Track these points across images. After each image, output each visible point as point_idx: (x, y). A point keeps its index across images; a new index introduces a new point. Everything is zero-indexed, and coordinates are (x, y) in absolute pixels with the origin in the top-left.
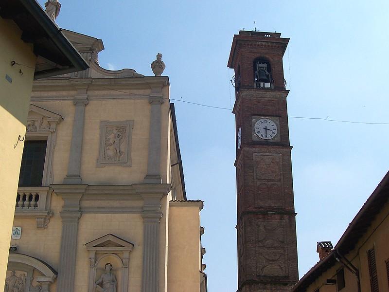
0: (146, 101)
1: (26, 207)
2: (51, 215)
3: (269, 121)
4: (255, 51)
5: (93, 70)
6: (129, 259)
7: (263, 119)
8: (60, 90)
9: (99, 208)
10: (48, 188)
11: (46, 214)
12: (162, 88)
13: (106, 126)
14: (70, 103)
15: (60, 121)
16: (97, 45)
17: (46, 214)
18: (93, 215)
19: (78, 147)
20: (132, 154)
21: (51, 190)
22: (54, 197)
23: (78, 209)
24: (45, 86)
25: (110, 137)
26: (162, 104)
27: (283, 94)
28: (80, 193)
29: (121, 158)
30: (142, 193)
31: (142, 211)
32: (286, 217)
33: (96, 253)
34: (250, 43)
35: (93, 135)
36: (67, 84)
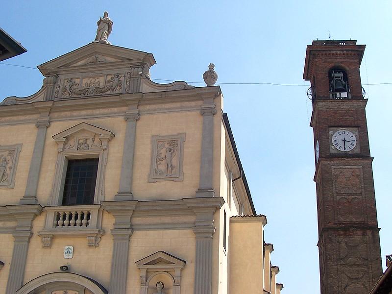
0: (199, 112)
1: (78, 226)
2: (102, 233)
3: (347, 132)
4: (330, 60)
5: (144, 84)
6: (181, 277)
7: (341, 131)
8: (112, 107)
9: (150, 225)
10: (99, 206)
11: (97, 232)
12: (214, 98)
13: (157, 140)
14: (121, 119)
15: (112, 138)
16: (147, 60)
17: (97, 232)
18: (144, 232)
19: (129, 163)
20: (184, 167)
21: (103, 208)
22: (106, 215)
23: (129, 226)
24: (96, 104)
25: (161, 151)
26: (214, 114)
27: (361, 103)
28: (129, 210)
29: (173, 173)
30: (193, 207)
31: (195, 227)
32: (369, 233)
33: (147, 272)
34: (324, 53)
35: (144, 151)
36: (118, 100)
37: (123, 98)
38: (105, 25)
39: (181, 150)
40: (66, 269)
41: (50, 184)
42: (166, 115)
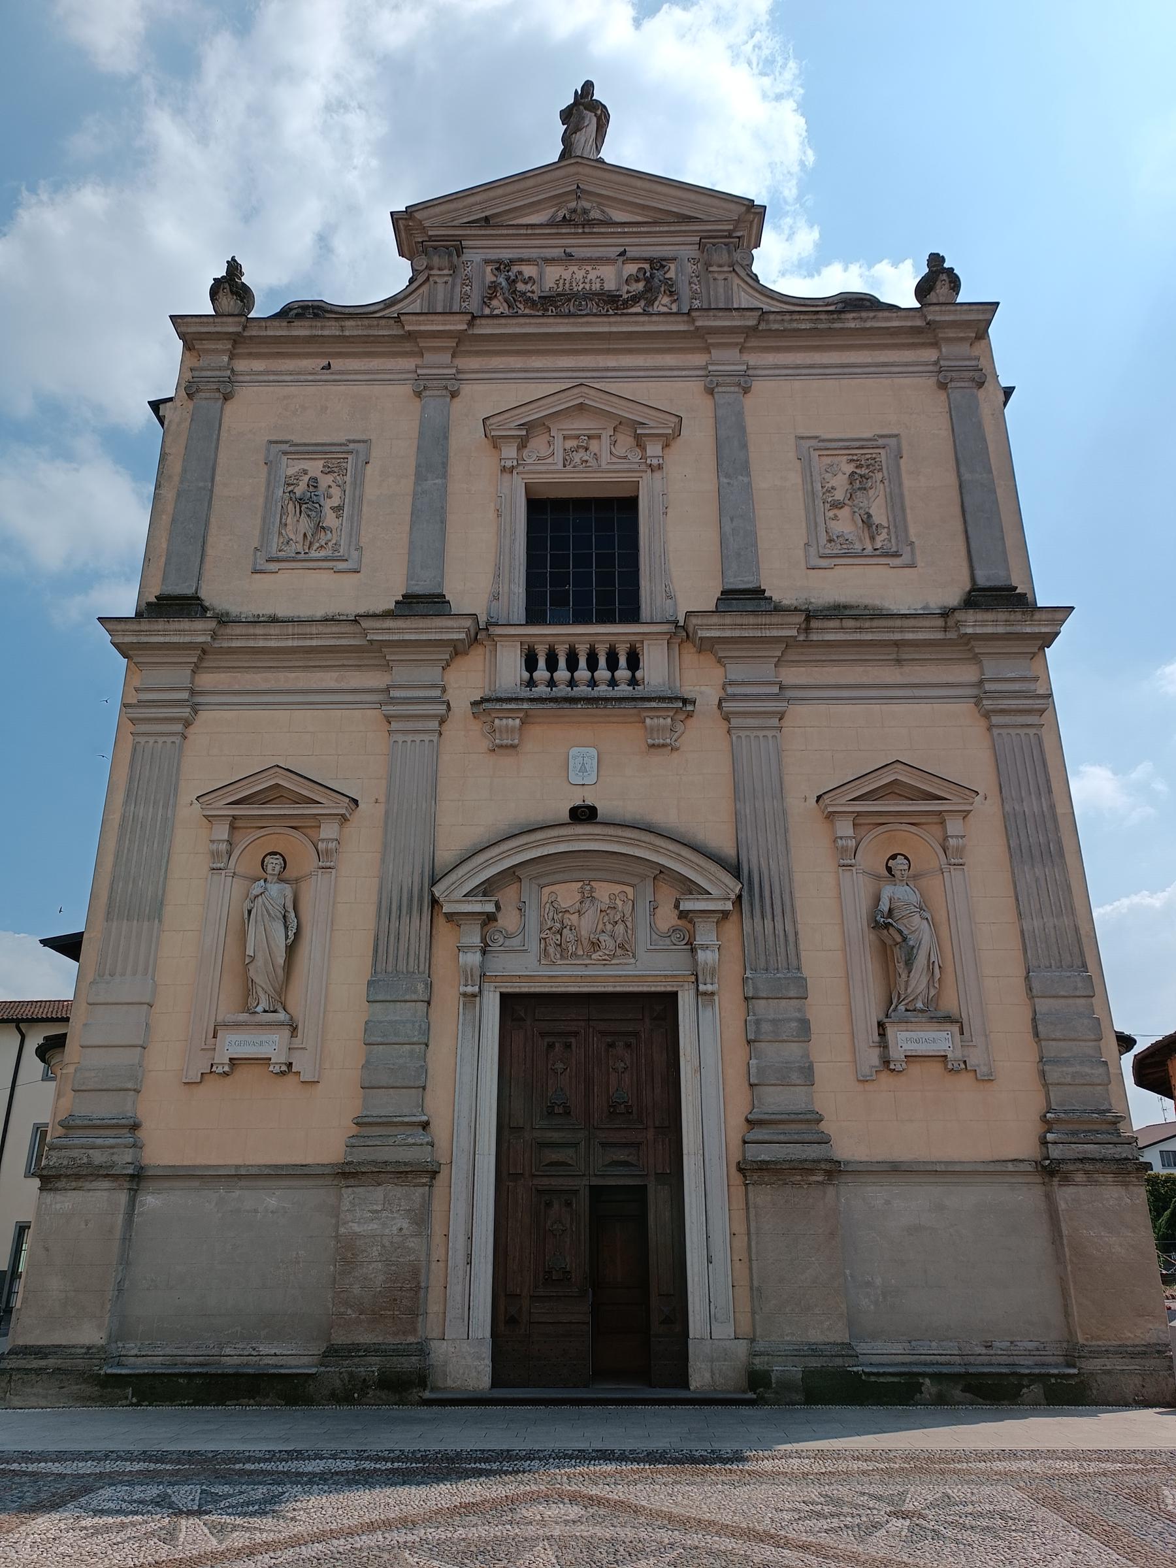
14: (696, 386)
31: (980, 695)
37: (699, 323)
38: (585, 113)
39: (896, 479)
40: (583, 814)
41: (484, 563)
42: (831, 383)
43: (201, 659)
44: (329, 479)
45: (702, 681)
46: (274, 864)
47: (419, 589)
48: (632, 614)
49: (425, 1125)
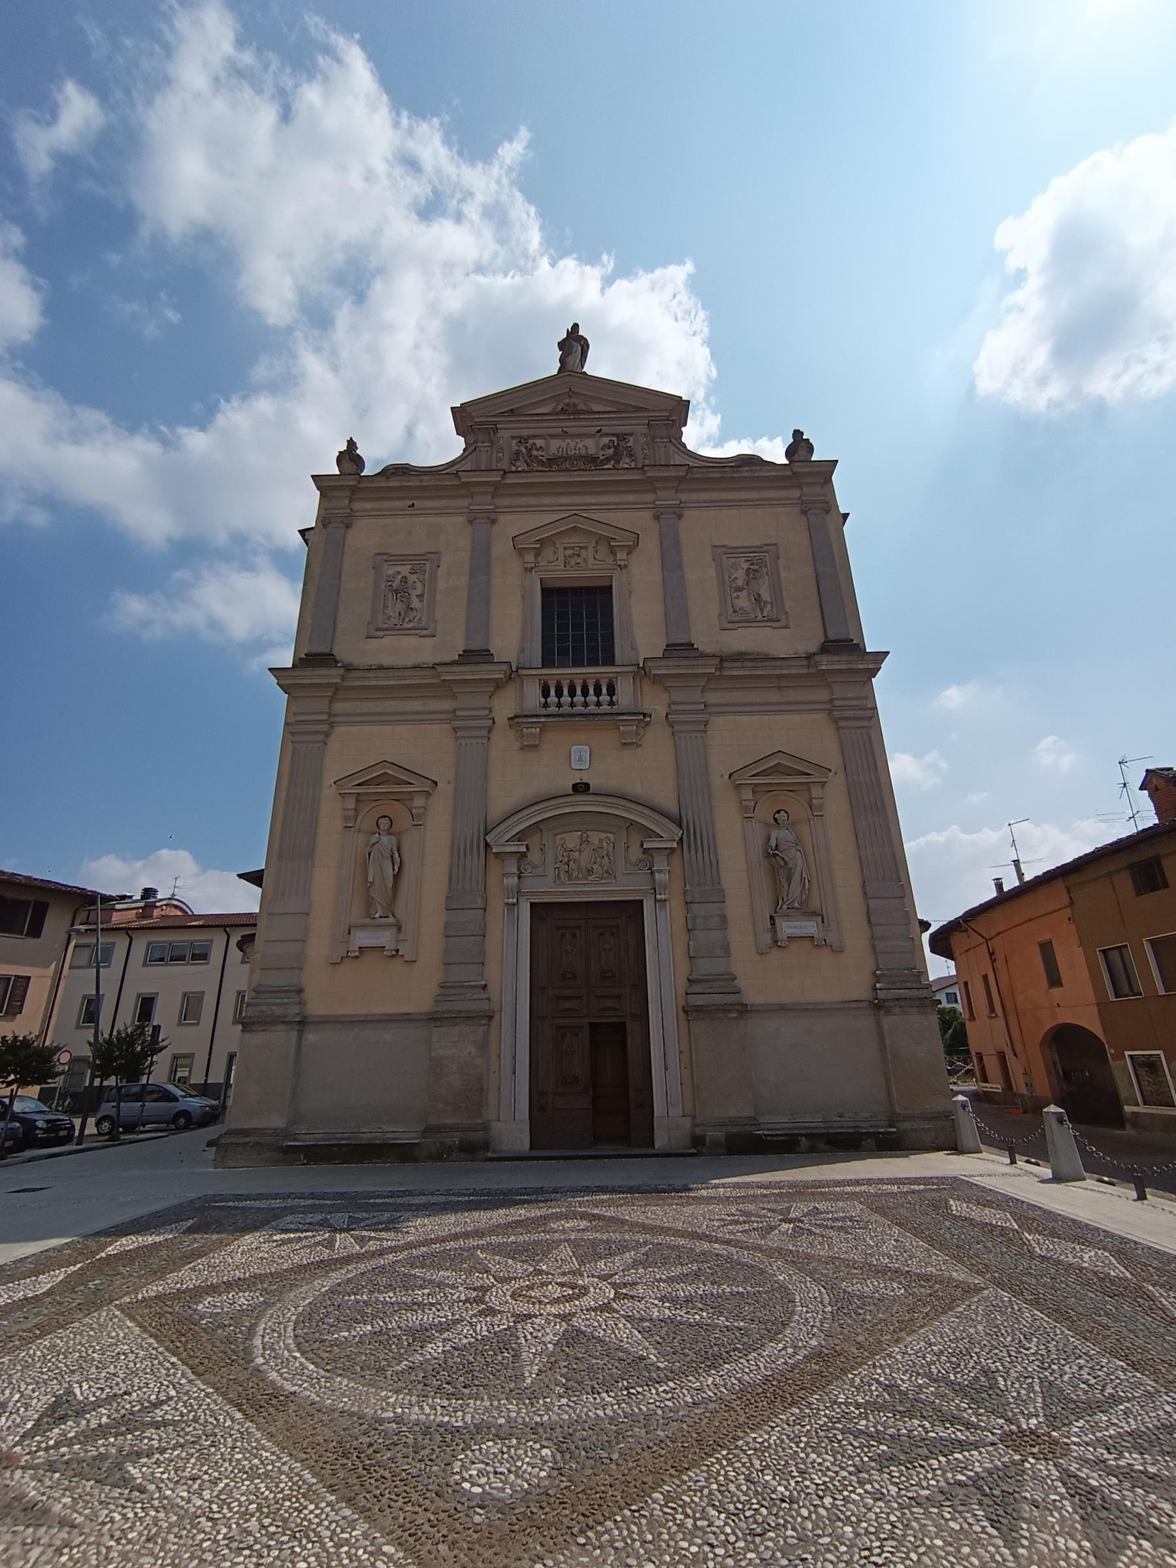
14: (647, 515)
18: (732, 718)
31: (831, 709)
38: (574, 345)
40: (581, 788)
41: (514, 629)
43: (335, 693)
44: (414, 577)
45: (655, 703)
46: (384, 823)
47: (473, 647)
48: (610, 660)
49: (484, 987)
